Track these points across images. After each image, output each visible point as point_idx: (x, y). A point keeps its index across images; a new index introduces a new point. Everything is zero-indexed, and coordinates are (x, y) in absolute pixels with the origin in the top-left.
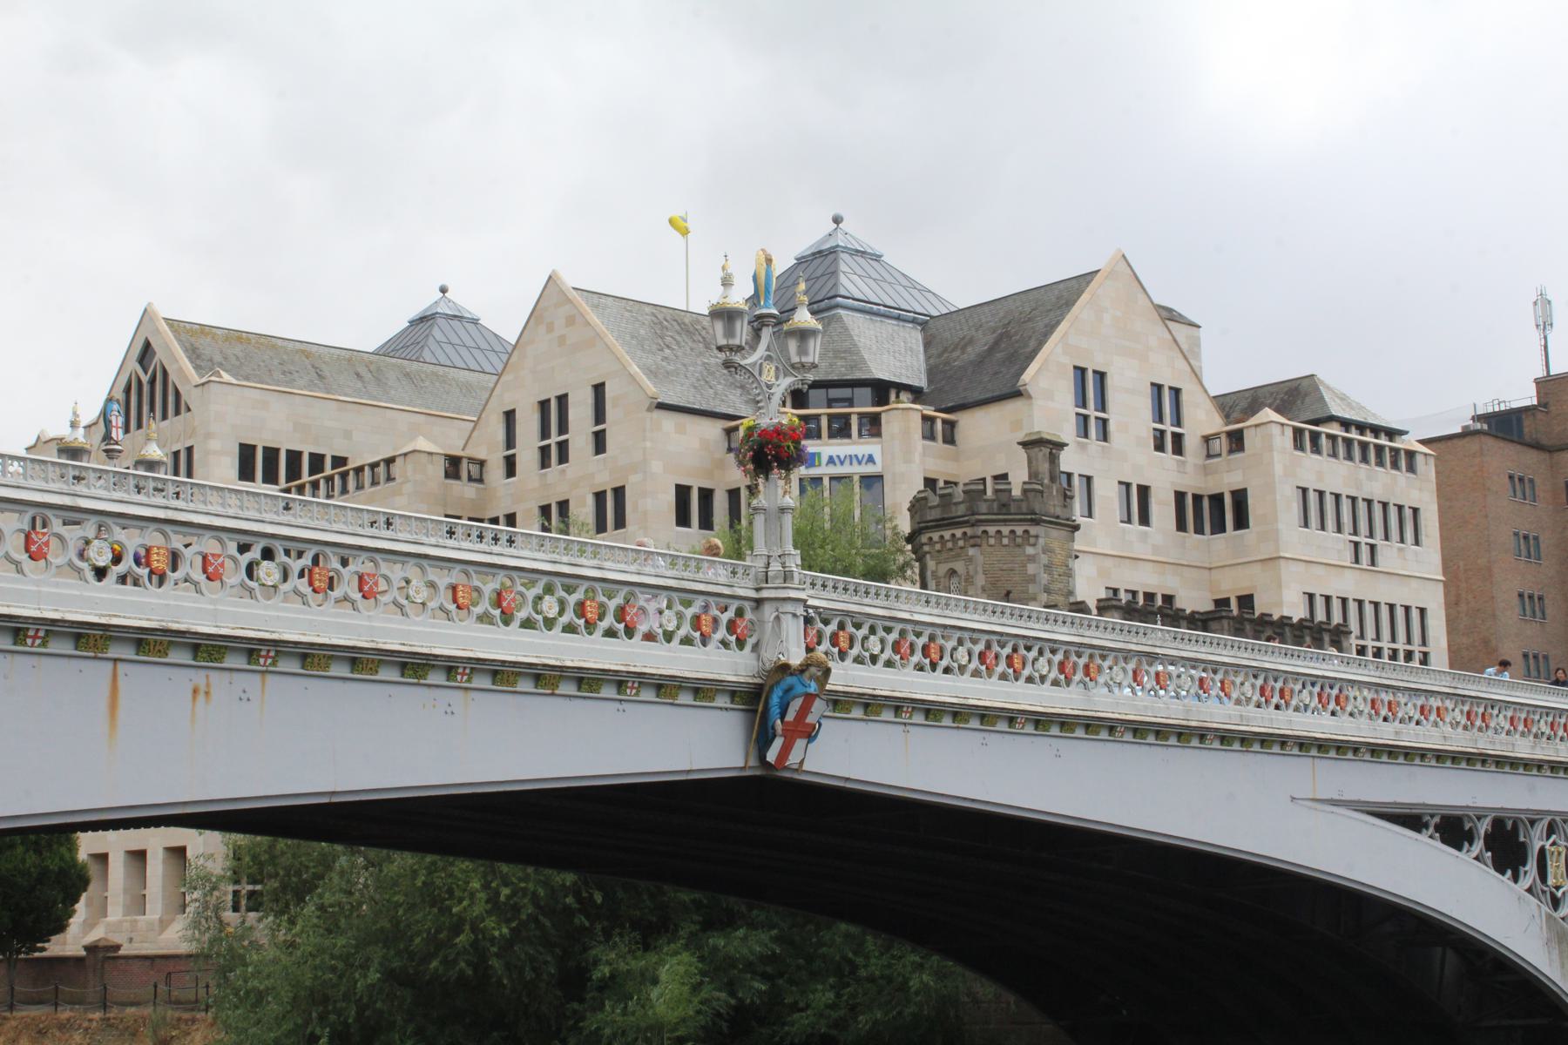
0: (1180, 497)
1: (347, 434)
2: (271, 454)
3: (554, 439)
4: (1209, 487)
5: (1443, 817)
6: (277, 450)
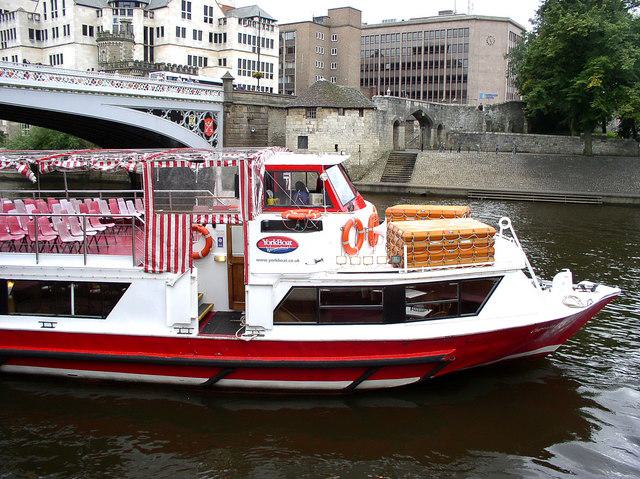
0: (211, 34)
1: (8, 4)
3: (55, 11)
4: (218, 32)
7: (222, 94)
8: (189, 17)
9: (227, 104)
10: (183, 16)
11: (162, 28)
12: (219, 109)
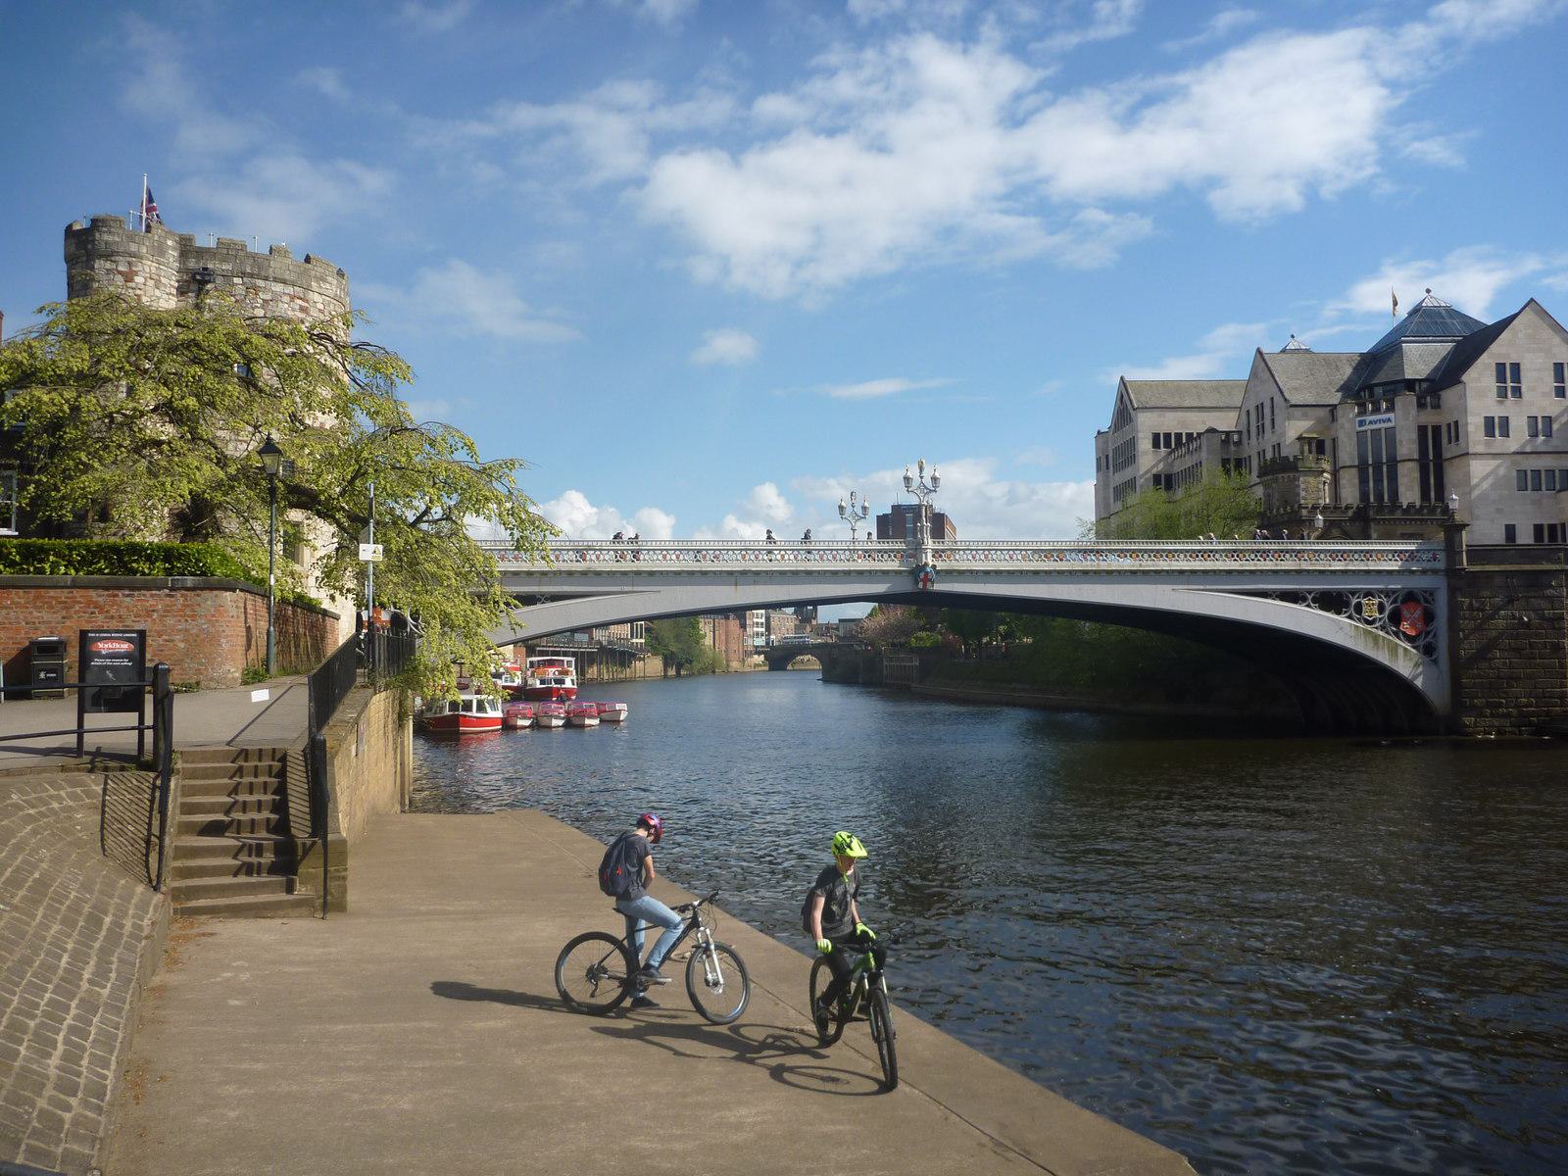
2: (1168, 436)
5: (1281, 593)
6: (1170, 434)
7: (1441, 556)
8: (1517, 392)
9: (1452, 573)
10: (1502, 394)
11: (1456, 423)
12: (1439, 584)
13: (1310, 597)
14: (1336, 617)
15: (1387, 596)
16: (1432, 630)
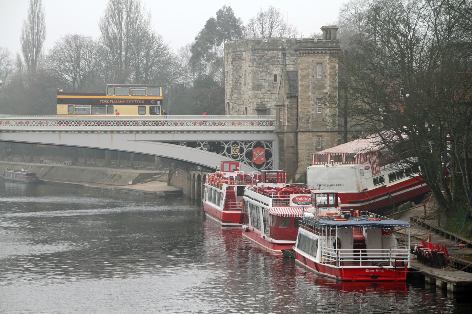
5: (187, 142)
13: (202, 145)
14: (216, 154)
15: (246, 144)
16: (270, 162)
